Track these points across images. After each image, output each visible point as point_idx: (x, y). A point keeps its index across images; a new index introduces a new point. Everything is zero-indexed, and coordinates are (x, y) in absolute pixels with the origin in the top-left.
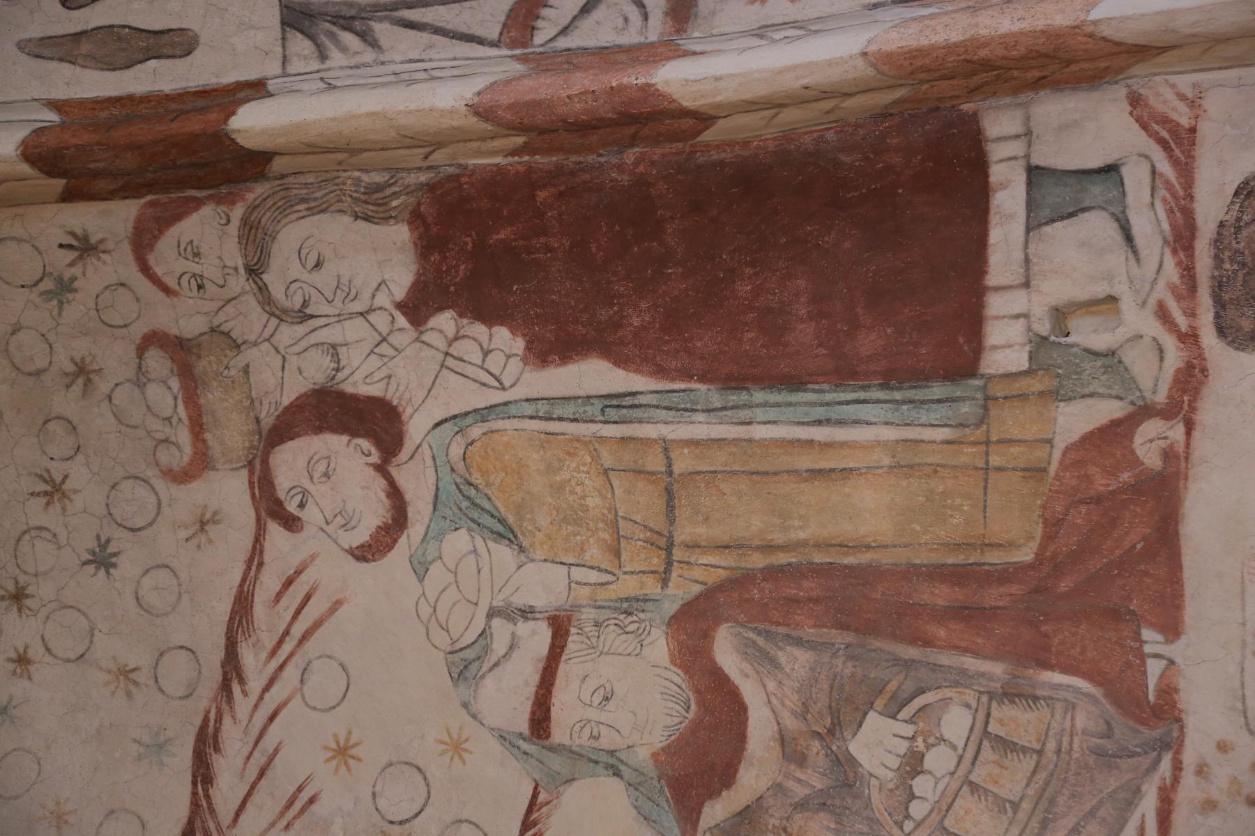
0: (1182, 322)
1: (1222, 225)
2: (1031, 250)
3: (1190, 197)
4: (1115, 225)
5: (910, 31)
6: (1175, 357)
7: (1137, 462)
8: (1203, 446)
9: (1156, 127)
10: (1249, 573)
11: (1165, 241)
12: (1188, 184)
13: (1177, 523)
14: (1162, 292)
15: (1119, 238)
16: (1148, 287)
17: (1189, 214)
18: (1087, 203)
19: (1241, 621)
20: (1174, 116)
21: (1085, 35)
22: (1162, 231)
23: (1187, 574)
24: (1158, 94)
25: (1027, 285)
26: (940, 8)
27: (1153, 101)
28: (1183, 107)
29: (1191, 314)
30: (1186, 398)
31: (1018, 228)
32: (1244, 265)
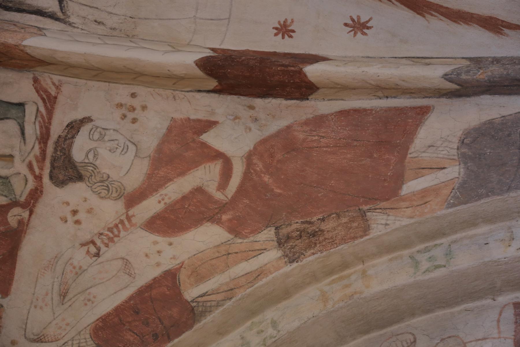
0: (37, 171)
1: (60, 137)
3: (50, 123)
4: (19, 127)
6: (31, 184)
7: (7, 223)
8: (35, 221)
9: (42, 93)
10: (41, 274)
11: (37, 138)
12: (50, 118)
13: (18, 250)
14: (31, 158)
15: (19, 133)
16: (26, 154)
17: (48, 130)
18: (9, 116)
19: (33, 293)
20: (50, 90)
21: (20, 50)
22: (36, 134)
23: (17, 271)
24: (45, 80)
27: (42, 83)
28: (53, 88)
30: (32, 201)
32: (65, 154)
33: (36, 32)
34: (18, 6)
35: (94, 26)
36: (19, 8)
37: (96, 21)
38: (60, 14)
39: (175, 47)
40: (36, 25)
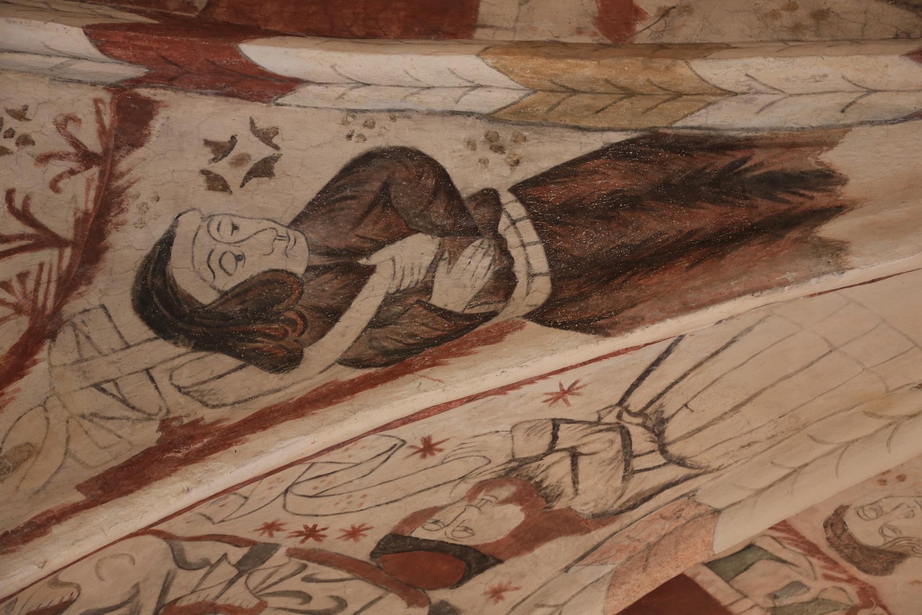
0: (844, 576)
2: (736, 586)
3: (797, 534)
4: (772, 561)
5: (621, 597)
6: (852, 590)
11: (804, 555)
15: (778, 564)
16: (811, 572)
18: (750, 562)
22: (799, 553)
25: (746, 596)
26: (614, 564)
29: (845, 572)
30: (871, 599)
31: (721, 583)
32: (855, 548)
33: (697, 512)
34: (639, 498)
35: (747, 452)
36: (644, 499)
37: (743, 447)
38: (693, 472)
39: (880, 414)
40: (680, 494)
